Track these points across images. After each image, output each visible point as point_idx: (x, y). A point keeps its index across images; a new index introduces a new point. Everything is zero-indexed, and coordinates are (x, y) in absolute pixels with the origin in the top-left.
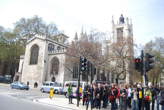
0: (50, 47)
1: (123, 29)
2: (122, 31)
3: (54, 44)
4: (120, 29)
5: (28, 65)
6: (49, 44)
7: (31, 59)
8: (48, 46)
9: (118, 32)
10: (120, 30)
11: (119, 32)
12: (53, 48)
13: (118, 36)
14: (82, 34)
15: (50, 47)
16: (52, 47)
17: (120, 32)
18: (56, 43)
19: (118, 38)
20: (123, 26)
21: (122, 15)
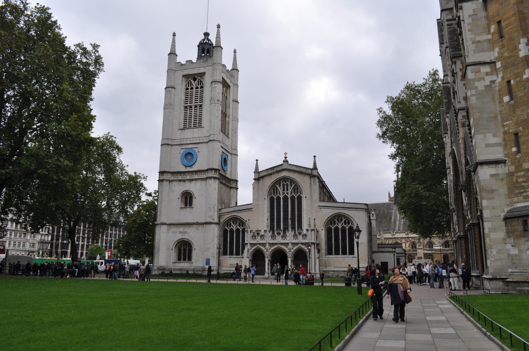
4: (195, 80)
9: (187, 89)
10: (193, 82)
13: (186, 102)
17: (194, 87)
19: (186, 107)
20: (201, 70)
21: (207, 34)
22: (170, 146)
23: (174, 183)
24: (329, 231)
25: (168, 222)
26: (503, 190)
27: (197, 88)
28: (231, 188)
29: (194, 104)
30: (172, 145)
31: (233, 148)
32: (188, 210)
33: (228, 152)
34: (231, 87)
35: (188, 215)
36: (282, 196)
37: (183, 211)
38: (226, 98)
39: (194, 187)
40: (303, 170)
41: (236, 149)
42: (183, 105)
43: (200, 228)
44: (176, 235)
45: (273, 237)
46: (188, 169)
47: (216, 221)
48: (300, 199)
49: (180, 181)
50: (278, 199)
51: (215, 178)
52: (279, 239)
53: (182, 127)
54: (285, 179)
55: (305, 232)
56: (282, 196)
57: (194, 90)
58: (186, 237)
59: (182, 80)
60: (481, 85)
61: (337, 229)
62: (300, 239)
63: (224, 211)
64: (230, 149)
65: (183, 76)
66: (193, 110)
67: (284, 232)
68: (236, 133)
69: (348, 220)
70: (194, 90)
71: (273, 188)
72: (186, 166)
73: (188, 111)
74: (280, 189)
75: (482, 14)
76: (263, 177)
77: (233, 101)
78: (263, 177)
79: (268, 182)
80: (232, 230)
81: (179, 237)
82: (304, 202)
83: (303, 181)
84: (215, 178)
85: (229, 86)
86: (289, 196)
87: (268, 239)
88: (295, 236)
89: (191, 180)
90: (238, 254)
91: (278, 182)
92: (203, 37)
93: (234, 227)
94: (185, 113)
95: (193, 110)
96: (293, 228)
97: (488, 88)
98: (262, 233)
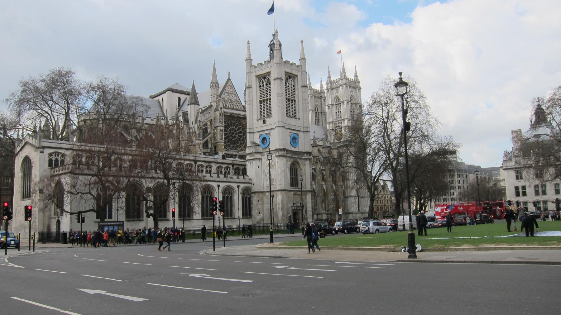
0: (54, 159)
1: (270, 76)
2: (268, 83)
3: (62, 151)
4: (265, 78)
5: (19, 199)
6: (51, 155)
7: (24, 187)
8: (47, 159)
9: (260, 86)
10: (263, 80)
11: (263, 86)
12: (63, 162)
14: (215, 85)
15: (54, 159)
16: (60, 160)
17: (265, 84)
18: (67, 149)
19: (260, 102)
22: (252, 134)
27: (267, 85)
29: (265, 99)
30: (253, 133)
31: (305, 126)
33: (300, 131)
34: (298, 76)
38: (294, 86)
42: (259, 99)
53: (259, 118)
57: (265, 86)
59: (256, 80)
64: (301, 128)
65: (257, 76)
66: (265, 103)
70: (265, 86)
73: (262, 104)
77: (302, 87)
85: (297, 76)
92: (272, 38)
94: (261, 106)
95: (265, 103)
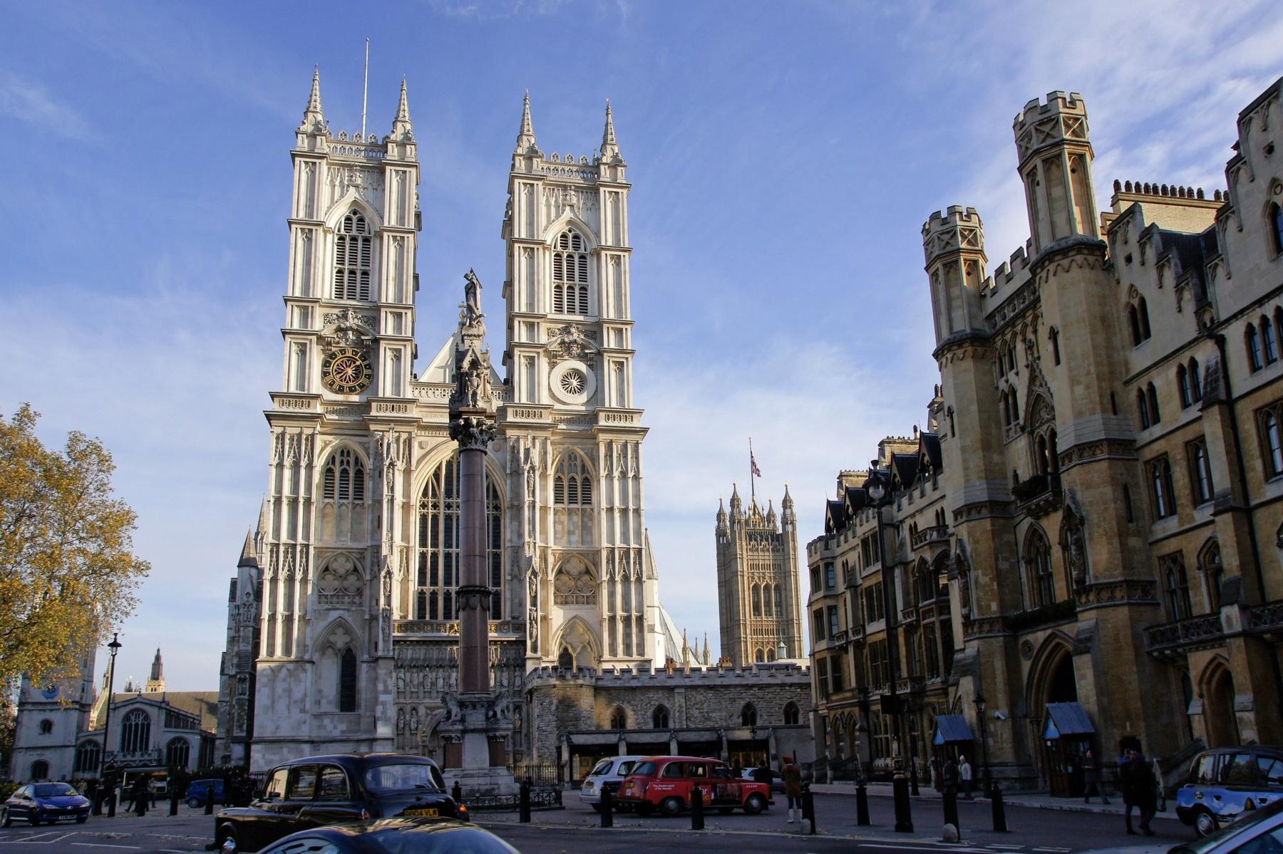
23: (34, 712)
24: (169, 749)
25: (25, 746)
26: (223, 747)
28: (85, 712)
32: (47, 735)
35: (46, 740)
36: (133, 723)
37: (41, 737)
39: (54, 717)
40: (154, 703)
41: (92, 677)
43: (58, 751)
44: (33, 757)
45: (124, 756)
46: (50, 700)
47: (74, 744)
48: (149, 725)
49: (40, 710)
50: (131, 725)
51: (76, 709)
52: (129, 758)
54: (137, 710)
55: (150, 752)
56: (133, 723)
58: (43, 758)
60: (222, 710)
61: (176, 748)
62: (146, 757)
63: (81, 735)
67: (134, 753)
68: (94, 661)
69: (186, 742)
71: (127, 717)
72: (47, 698)
74: (133, 718)
75: (227, 682)
76: (119, 707)
78: (119, 707)
79: (123, 711)
80: (86, 751)
81: (35, 758)
82: (152, 728)
83: (153, 712)
84: (76, 709)
86: (140, 723)
87: (120, 758)
88: (142, 755)
89: (51, 710)
90: (90, 769)
91: (132, 712)
93: (89, 748)
96: (141, 750)
97: (225, 711)
98: (116, 753)
